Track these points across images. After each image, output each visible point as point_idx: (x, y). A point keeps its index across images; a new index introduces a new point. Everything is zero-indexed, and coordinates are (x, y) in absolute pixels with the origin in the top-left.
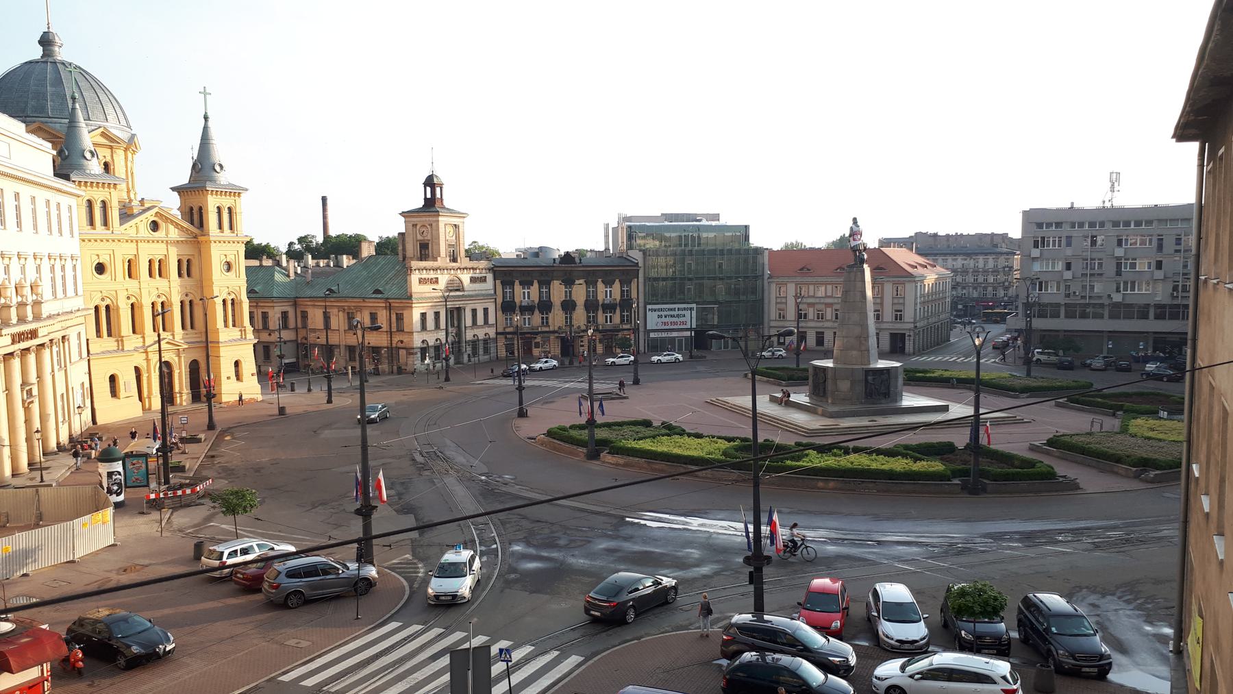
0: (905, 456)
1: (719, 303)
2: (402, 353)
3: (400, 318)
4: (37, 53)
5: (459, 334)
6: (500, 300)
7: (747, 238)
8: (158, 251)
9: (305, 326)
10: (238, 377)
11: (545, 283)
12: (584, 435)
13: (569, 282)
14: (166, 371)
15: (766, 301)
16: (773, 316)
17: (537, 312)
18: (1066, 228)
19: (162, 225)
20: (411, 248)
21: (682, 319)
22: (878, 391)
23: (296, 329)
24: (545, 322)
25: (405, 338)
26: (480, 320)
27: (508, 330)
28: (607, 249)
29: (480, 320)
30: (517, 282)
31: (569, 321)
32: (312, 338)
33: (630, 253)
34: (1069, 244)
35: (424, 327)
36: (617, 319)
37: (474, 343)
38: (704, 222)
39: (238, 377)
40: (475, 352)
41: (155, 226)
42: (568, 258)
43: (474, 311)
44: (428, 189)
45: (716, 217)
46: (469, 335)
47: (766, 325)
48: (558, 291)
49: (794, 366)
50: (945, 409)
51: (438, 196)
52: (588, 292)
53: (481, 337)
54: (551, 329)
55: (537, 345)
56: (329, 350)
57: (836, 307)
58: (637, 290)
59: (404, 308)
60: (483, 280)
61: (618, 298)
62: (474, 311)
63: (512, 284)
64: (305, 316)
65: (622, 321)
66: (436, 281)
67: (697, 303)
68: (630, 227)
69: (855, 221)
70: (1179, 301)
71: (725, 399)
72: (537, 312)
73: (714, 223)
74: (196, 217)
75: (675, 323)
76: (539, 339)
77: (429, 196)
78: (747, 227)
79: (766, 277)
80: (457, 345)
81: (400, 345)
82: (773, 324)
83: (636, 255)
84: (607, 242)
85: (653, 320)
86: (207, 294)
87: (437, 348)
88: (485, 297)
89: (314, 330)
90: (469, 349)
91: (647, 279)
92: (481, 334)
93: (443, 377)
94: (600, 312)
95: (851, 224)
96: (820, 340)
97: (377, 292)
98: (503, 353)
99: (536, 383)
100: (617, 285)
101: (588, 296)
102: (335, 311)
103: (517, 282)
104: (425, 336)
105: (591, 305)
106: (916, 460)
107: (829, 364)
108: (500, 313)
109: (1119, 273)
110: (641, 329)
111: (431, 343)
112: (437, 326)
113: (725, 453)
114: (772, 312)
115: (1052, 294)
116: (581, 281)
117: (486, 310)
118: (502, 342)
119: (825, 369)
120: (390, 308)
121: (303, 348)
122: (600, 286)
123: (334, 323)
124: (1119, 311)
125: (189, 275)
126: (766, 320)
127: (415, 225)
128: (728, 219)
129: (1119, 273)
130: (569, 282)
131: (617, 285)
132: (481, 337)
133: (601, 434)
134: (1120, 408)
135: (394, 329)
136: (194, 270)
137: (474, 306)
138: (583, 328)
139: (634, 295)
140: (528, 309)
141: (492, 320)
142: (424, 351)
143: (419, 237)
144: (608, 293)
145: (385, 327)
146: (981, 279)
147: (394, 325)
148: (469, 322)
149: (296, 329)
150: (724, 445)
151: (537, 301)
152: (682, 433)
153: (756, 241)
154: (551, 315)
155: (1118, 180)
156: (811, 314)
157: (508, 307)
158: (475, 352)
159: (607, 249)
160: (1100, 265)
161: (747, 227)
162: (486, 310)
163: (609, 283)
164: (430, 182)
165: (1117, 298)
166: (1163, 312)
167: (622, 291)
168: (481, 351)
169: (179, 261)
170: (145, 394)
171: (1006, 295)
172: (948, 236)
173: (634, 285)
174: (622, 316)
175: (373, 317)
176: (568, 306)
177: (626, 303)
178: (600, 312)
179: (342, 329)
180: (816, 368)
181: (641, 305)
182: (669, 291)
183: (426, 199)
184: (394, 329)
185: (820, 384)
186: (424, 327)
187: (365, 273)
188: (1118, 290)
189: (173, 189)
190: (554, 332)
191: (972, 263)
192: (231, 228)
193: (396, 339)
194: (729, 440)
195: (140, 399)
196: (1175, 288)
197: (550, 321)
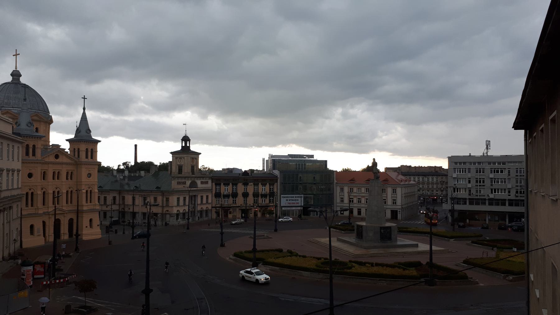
0: (399, 267)
2: (168, 216)
3: (167, 200)
4: (9, 79)
5: (194, 207)
6: (214, 192)
8: (57, 168)
10: (91, 226)
12: (251, 256)
13: (246, 184)
14: (57, 224)
15: (335, 195)
16: (338, 202)
17: (231, 197)
18: (468, 164)
20: (175, 169)
21: (297, 202)
22: (386, 235)
23: (119, 205)
24: (234, 202)
25: (170, 209)
26: (204, 201)
28: (264, 169)
29: (204, 201)
30: (222, 184)
31: (245, 202)
33: (274, 171)
34: (469, 172)
35: (178, 205)
36: (267, 201)
37: (201, 212)
38: (307, 158)
39: (91, 226)
40: (201, 214)
41: (57, 157)
43: (202, 197)
44: (184, 142)
45: (312, 156)
46: (199, 208)
47: (335, 205)
48: (241, 188)
50: (417, 246)
51: (188, 145)
52: (254, 189)
55: (230, 213)
56: (134, 214)
57: (367, 198)
60: (207, 183)
61: (268, 192)
62: (202, 197)
63: (220, 185)
64: (124, 198)
65: (270, 202)
66: (185, 183)
67: (304, 194)
69: (374, 159)
70: (519, 198)
71: (316, 239)
72: (231, 197)
75: (294, 203)
76: (231, 210)
77: (184, 145)
78: (326, 161)
79: (335, 183)
81: (167, 212)
82: (338, 205)
83: (276, 172)
84: (264, 167)
85: (284, 202)
86: (79, 233)
87: (184, 214)
90: (199, 215)
91: (281, 183)
92: (204, 207)
93: (186, 227)
95: (372, 161)
96: (359, 213)
97: (157, 188)
99: (229, 230)
100: (268, 185)
101: (254, 190)
102: (138, 196)
103: (222, 184)
104: (178, 208)
105: (256, 195)
106: (404, 269)
107: (364, 224)
108: (214, 198)
109: (492, 185)
110: (278, 206)
111: (181, 212)
112: (184, 204)
113: (317, 266)
115: (462, 194)
116: (252, 184)
118: (214, 210)
119: (362, 226)
122: (260, 185)
123: (137, 202)
124: (492, 202)
125: (71, 179)
129: (492, 185)
130: (246, 184)
131: (268, 185)
133: (258, 255)
134: (495, 246)
135: (164, 205)
136: (74, 177)
137: (202, 195)
138: (252, 205)
139: (275, 190)
140: (227, 196)
141: (210, 201)
142: (177, 215)
143: (178, 163)
144: (264, 189)
146: (430, 187)
147: (165, 203)
148: (199, 202)
149: (119, 205)
150: (314, 261)
151: (231, 192)
152: (297, 255)
154: (237, 199)
155: (489, 144)
156: (355, 200)
157: (218, 195)
158: (201, 214)
159: (264, 169)
160: (483, 182)
161: (326, 161)
163: (264, 185)
165: (492, 196)
166: (512, 203)
167: (270, 188)
168: (204, 215)
170: (47, 235)
171: (442, 194)
172: (415, 167)
173: (275, 186)
174: (270, 200)
175: (155, 199)
176: (245, 195)
177: (272, 194)
179: (140, 205)
180: (358, 226)
183: (182, 146)
185: (360, 233)
186: (178, 205)
188: (492, 193)
189: (67, 140)
191: (426, 179)
192: (92, 158)
193: (165, 209)
194: (319, 259)
195: (44, 236)
196: (517, 192)
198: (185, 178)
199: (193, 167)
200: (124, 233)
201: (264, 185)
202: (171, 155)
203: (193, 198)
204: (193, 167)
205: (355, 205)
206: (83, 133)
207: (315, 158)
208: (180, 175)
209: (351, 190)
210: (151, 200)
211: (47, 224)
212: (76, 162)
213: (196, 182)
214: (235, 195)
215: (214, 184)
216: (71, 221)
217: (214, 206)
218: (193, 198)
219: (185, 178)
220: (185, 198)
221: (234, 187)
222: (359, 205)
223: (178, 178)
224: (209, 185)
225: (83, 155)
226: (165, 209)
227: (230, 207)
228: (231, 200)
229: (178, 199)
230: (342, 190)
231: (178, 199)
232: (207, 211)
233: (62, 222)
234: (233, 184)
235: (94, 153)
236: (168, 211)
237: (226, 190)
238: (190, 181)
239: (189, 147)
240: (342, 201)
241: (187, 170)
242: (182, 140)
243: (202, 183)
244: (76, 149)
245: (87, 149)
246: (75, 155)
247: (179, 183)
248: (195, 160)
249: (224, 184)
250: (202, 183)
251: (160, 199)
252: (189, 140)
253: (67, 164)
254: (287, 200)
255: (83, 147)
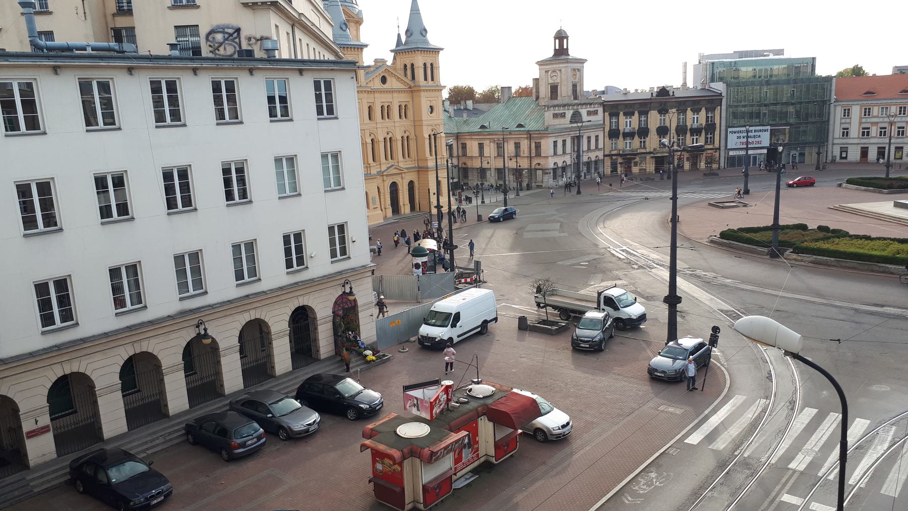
1: (790, 125)
2: (539, 173)
3: (538, 146)
5: (578, 157)
6: (607, 129)
7: (813, 67)
8: (385, 99)
9: (465, 154)
11: (644, 113)
13: (663, 111)
15: (831, 122)
17: (636, 137)
19: (389, 79)
20: (545, 91)
21: (757, 139)
23: (458, 157)
25: (542, 161)
26: (593, 147)
27: (613, 153)
28: (685, 84)
29: (593, 147)
30: (621, 114)
32: (469, 164)
33: (713, 85)
37: (588, 164)
38: (771, 57)
41: (384, 80)
42: (663, 92)
43: (589, 138)
44: (557, 41)
45: (781, 52)
46: (585, 159)
47: (830, 142)
49: (884, 176)
52: (679, 119)
53: (593, 159)
54: (648, 150)
55: (636, 164)
58: (720, 116)
59: (541, 138)
60: (596, 113)
61: (704, 123)
62: (589, 138)
63: (617, 115)
64: (464, 146)
65: (706, 142)
66: (563, 115)
67: (771, 125)
68: (713, 63)
72: (636, 137)
73: (781, 57)
74: (409, 72)
76: (637, 159)
79: (832, 101)
80: (577, 165)
81: (538, 167)
82: (836, 141)
84: (685, 78)
87: (564, 169)
88: (597, 127)
89: (472, 157)
90: (585, 169)
91: (728, 106)
92: (593, 156)
94: (688, 135)
97: (520, 126)
98: (608, 171)
100: (703, 111)
101: (679, 122)
102: (488, 142)
103: (621, 114)
108: (607, 139)
110: (722, 148)
111: (560, 165)
112: (564, 152)
114: (836, 131)
116: (674, 110)
117: (597, 137)
120: (530, 138)
121: (464, 171)
122: (689, 113)
123: (486, 152)
126: (830, 138)
127: (547, 72)
128: (794, 52)
130: (663, 111)
131: (703, 111)
132: (593, 159)
135: (533, 155)
136: (410, 113)
137: (597, 133)
139: (717, 121)
140: (629, 135)
141: (601, 145)
142: (554, 170)
143: (550, 81)
145: (526, 154)
147: (533, 151)
149: (458, 157)
151: (637, 128)
152: (845, 234)
153: (822, 71)
154: (647, 139)
156: (874, 131)
157: (614, 134)
159: (685, 84)
161: (814, 59)
162: (597, 137)
163: (696, 111)
164: (561, 37)
167: (707, 117)
168: (593, 170)
169: (400, 106)
173: (717, 112)
174: (706, 138)
175: (517, 146)
177: (710, 127)
178: (688, 135)
181: (723, 128)
182: (747, 114)
183: (555, 49)
184: (533, 155)
186: (555, 154)
187: (507, 112)
190: (650, 153)
192: (433, 80)
193: (535, 162)
197: (647, 144)
198: (564, 106)
199: (575, 86)
200: (483, 202)
201: (696, 111)
202: (537, 67)
203: (577, 140)
204: (575, 86)
205: (872, 141)
206: (416, 36)
207: (786, 56)
208: (555, 102)
209: (867, 112)
210: (510, 148)
211: (382, 190)
212: (410, 87)
213: (579, 113)
214: (643, 132)
215: (607, 114)
216: (411, 184)
217: (607, 153)
218: (577, 140)
219: (564, 106)
220: (564, 141)
221: (614, 120)
222: (880, 141)
223: (554, 106)
224: (599, 118)
225: (420, 73)
226: (535, 162)
227: (636, 155)
228: (637, 140)
229: (555, 142)
230: (847, 113)
231: (555, 142)
232: (596, 162)
233: (400, 187)
234: (640, 114)
235: (435, 71)
236: (539, 164)
237: (627, 123)
238: (571, 112)
239: (567, 49)
240: (846, 133)
241: (565, 91)
242: (555, 38)
243: (589, 113)
244: (409, 67)
245: (425, 64)
246: (406, 75)
247: (555, 116)
248: (578, 73)
249: (625, 114)
250: (589, 113)
251: (524, 144)
252: (567, 38)
253: (399, 91)
254: (738, 138)
255: (419, 60)
